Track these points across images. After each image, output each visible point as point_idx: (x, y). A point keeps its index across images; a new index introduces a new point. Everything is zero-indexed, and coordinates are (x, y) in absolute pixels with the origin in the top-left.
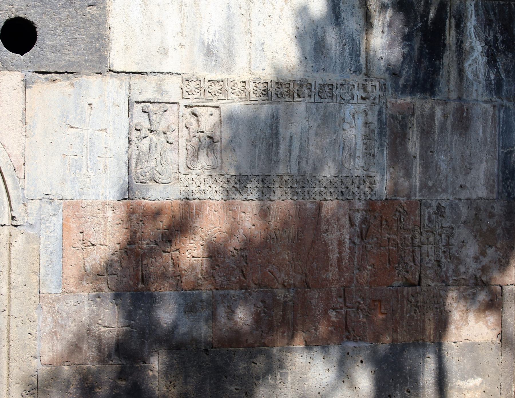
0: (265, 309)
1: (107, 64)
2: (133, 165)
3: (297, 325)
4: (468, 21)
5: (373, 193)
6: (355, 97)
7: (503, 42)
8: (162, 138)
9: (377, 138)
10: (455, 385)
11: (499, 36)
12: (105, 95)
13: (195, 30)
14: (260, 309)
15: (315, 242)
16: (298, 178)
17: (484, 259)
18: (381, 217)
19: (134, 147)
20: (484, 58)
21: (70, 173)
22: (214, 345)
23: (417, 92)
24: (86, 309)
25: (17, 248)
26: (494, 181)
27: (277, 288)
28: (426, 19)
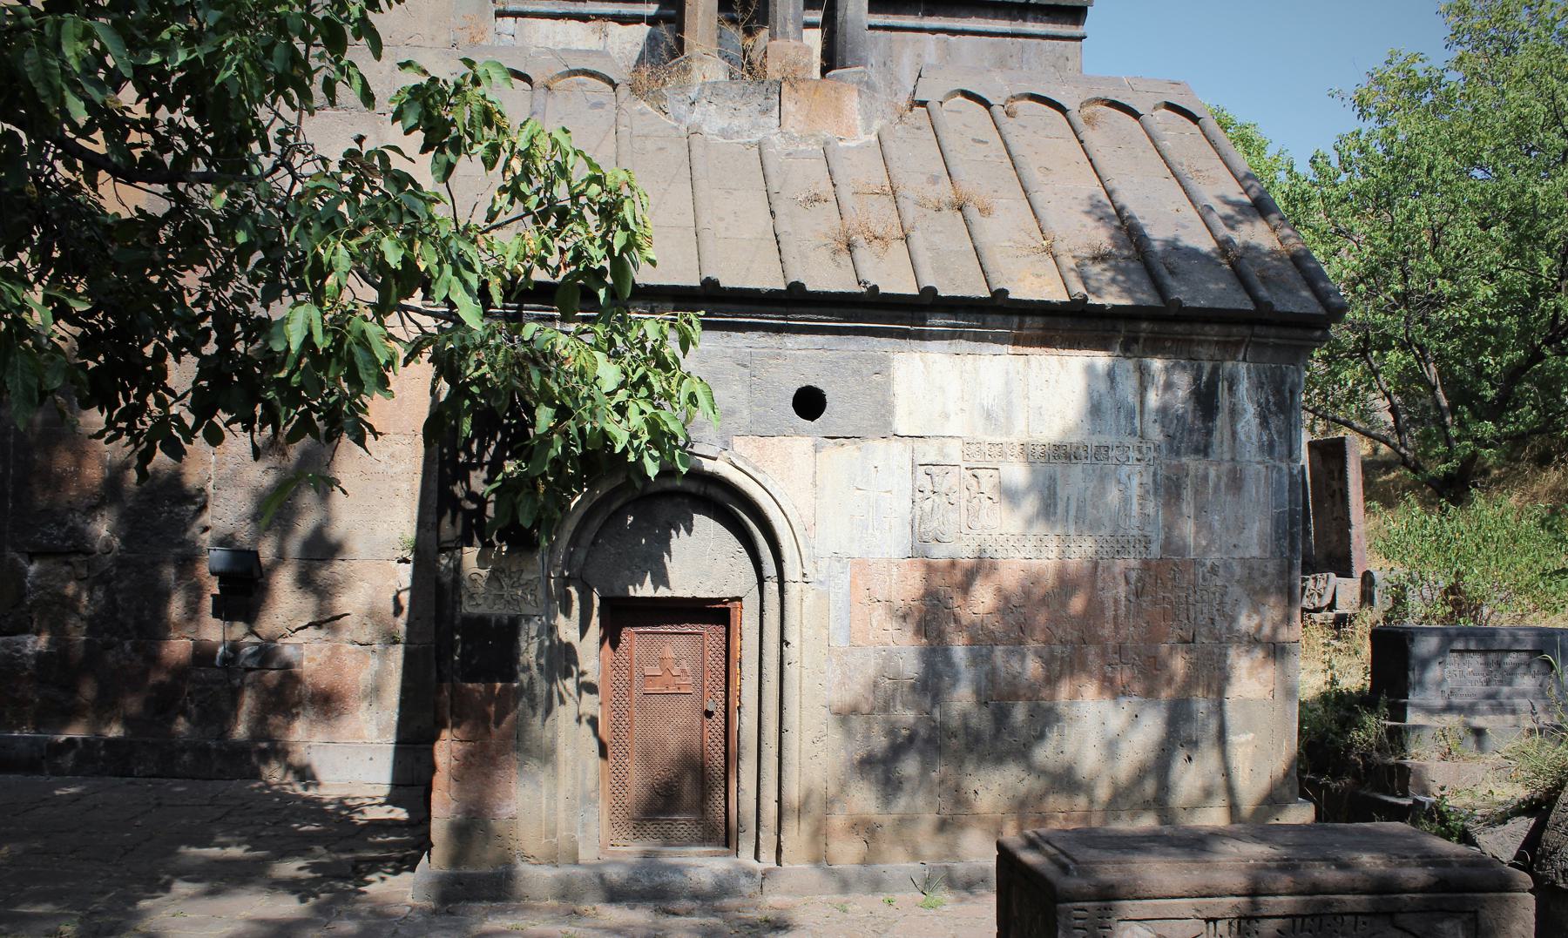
8: (944, 499)
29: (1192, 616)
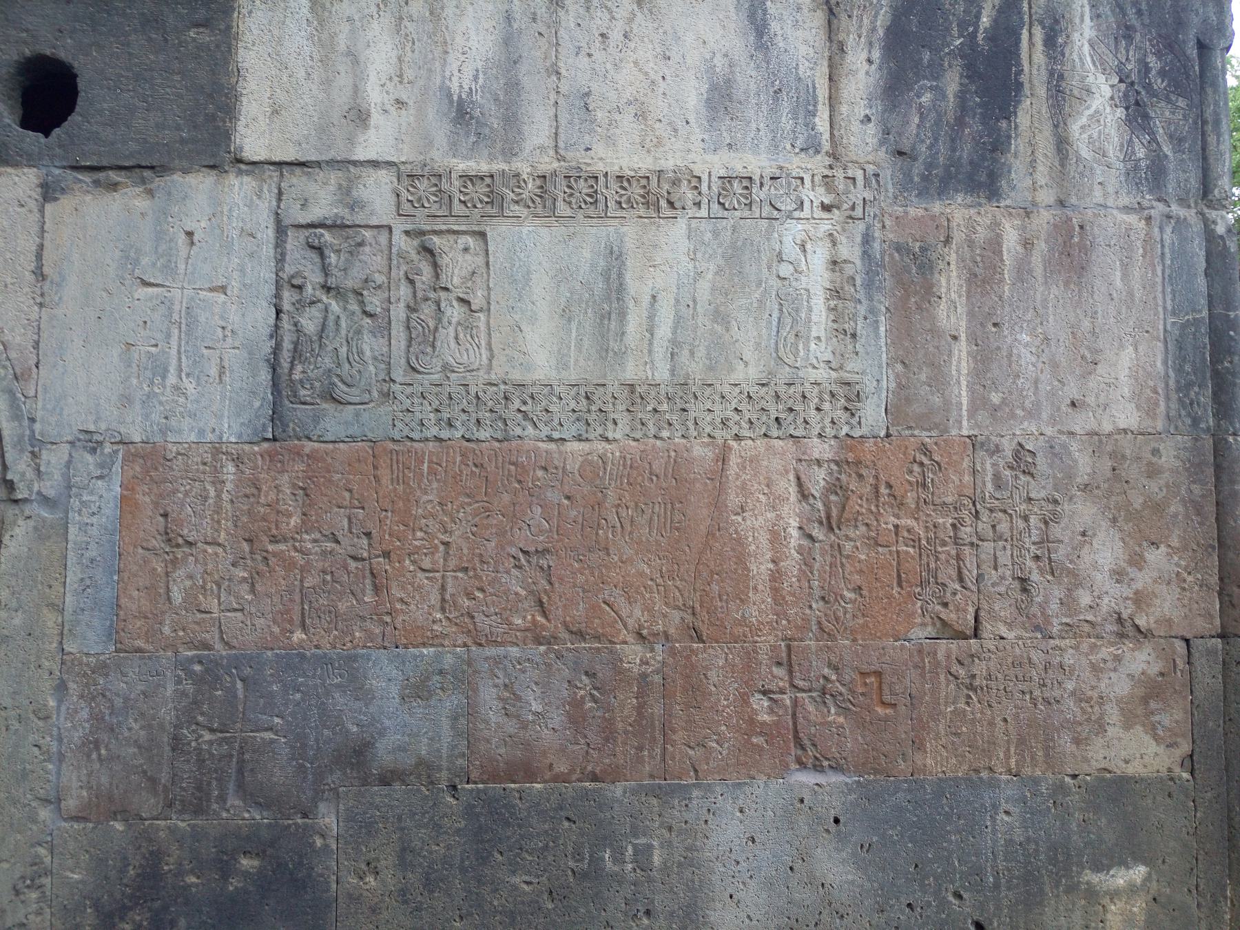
0: (595, 692)
1: (229, 146)
2: (286, 365)
3: (674, 731)
4: (1073, 30)
5: (854, 421)
6: (807, 205)
7: (1162, 73)
8: (354, 307)
9: (861, 295)
10: (1079, 882)
11: (1152, 61)
12: (222, 212)
13: (430, 70)
14: (582, 692)
15: (714, 535)
16: (670, 390)
17: (1139, 575)
18: (876, 477)
19: (286, 324)
20: (1119, 110)
21: (141, 383)
22: (472, 776)
23: (957, 191)
24: (170, 690)
25: (12, 550)
26: (1156, 393)
27: (625, 643)
28: (971, 29)
29: (971, 574)
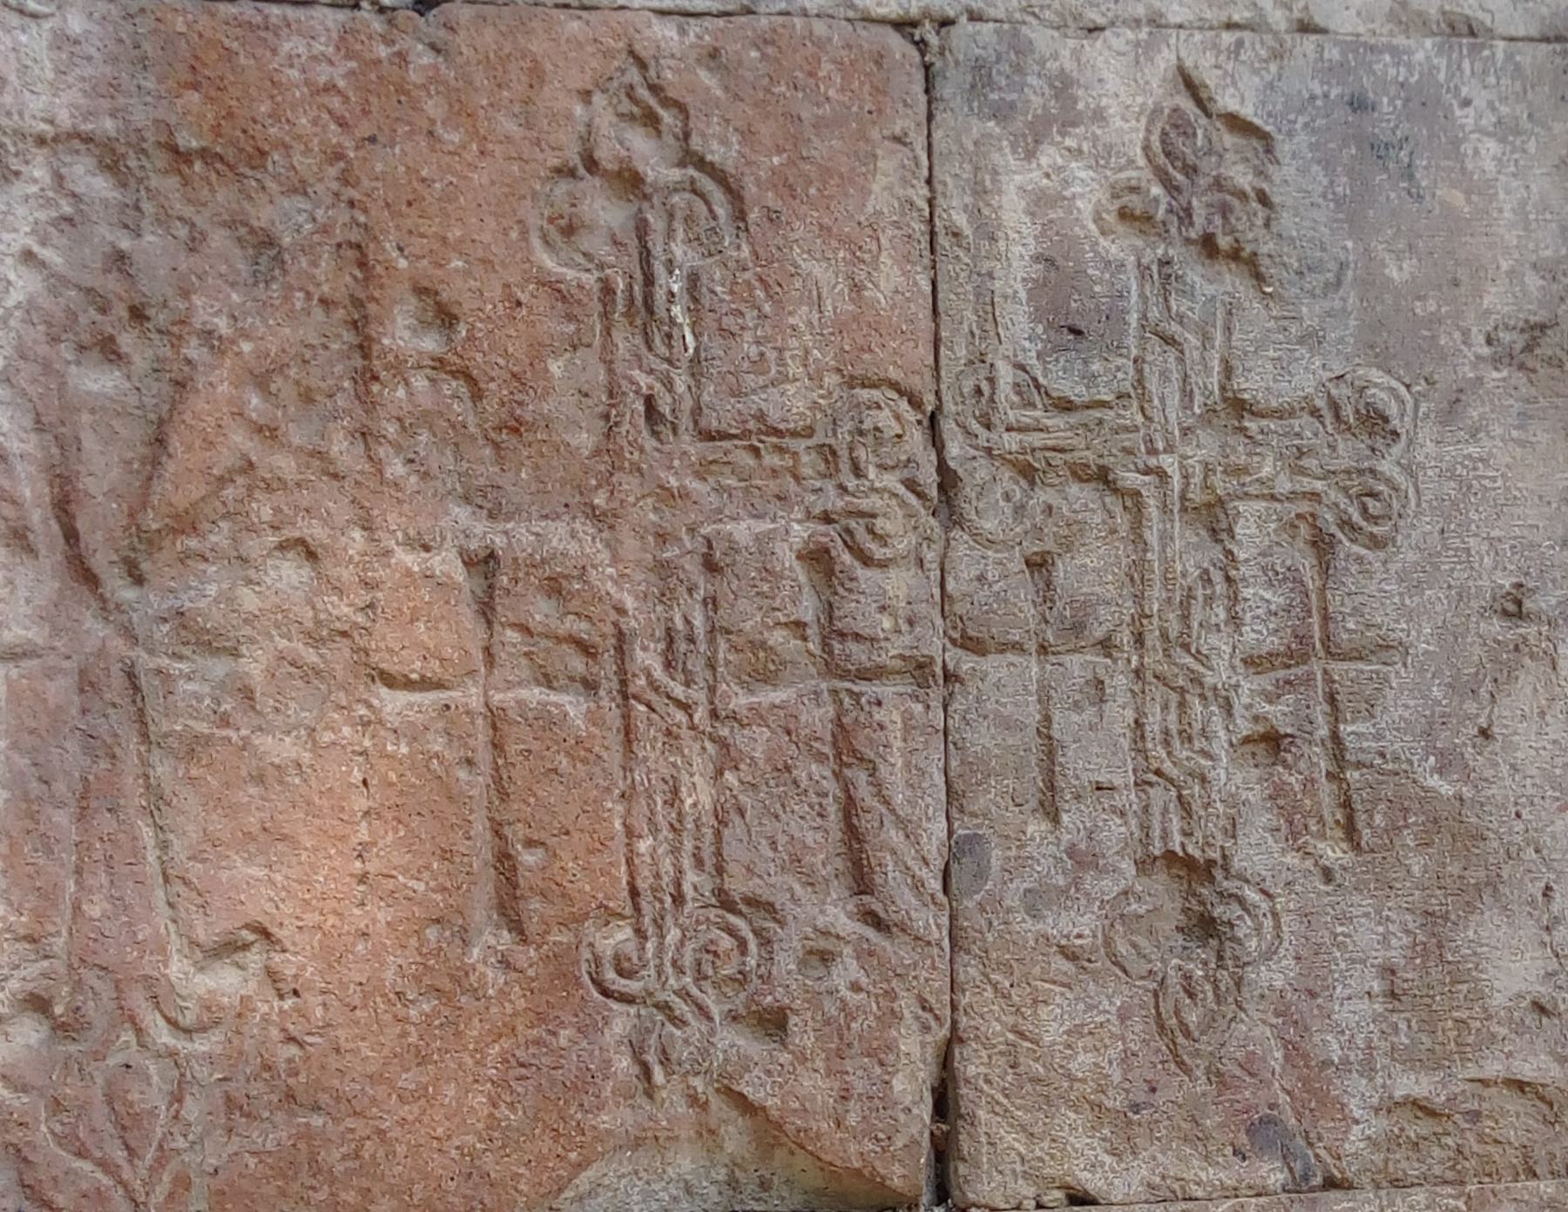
29: (911, 852)
